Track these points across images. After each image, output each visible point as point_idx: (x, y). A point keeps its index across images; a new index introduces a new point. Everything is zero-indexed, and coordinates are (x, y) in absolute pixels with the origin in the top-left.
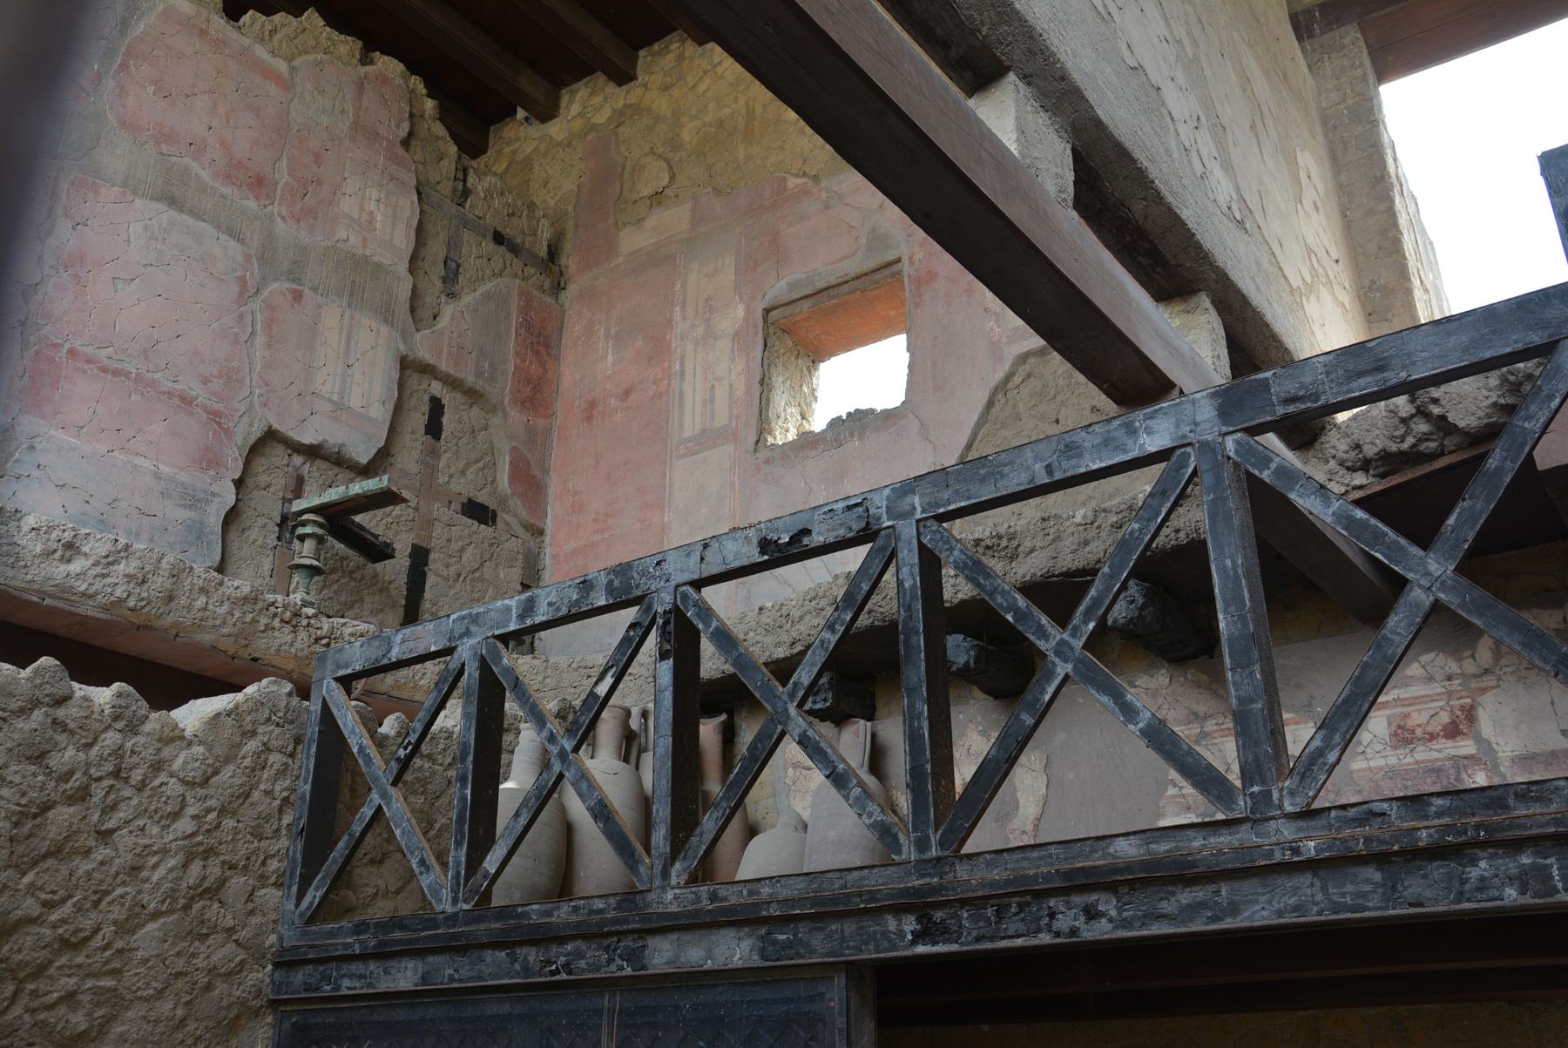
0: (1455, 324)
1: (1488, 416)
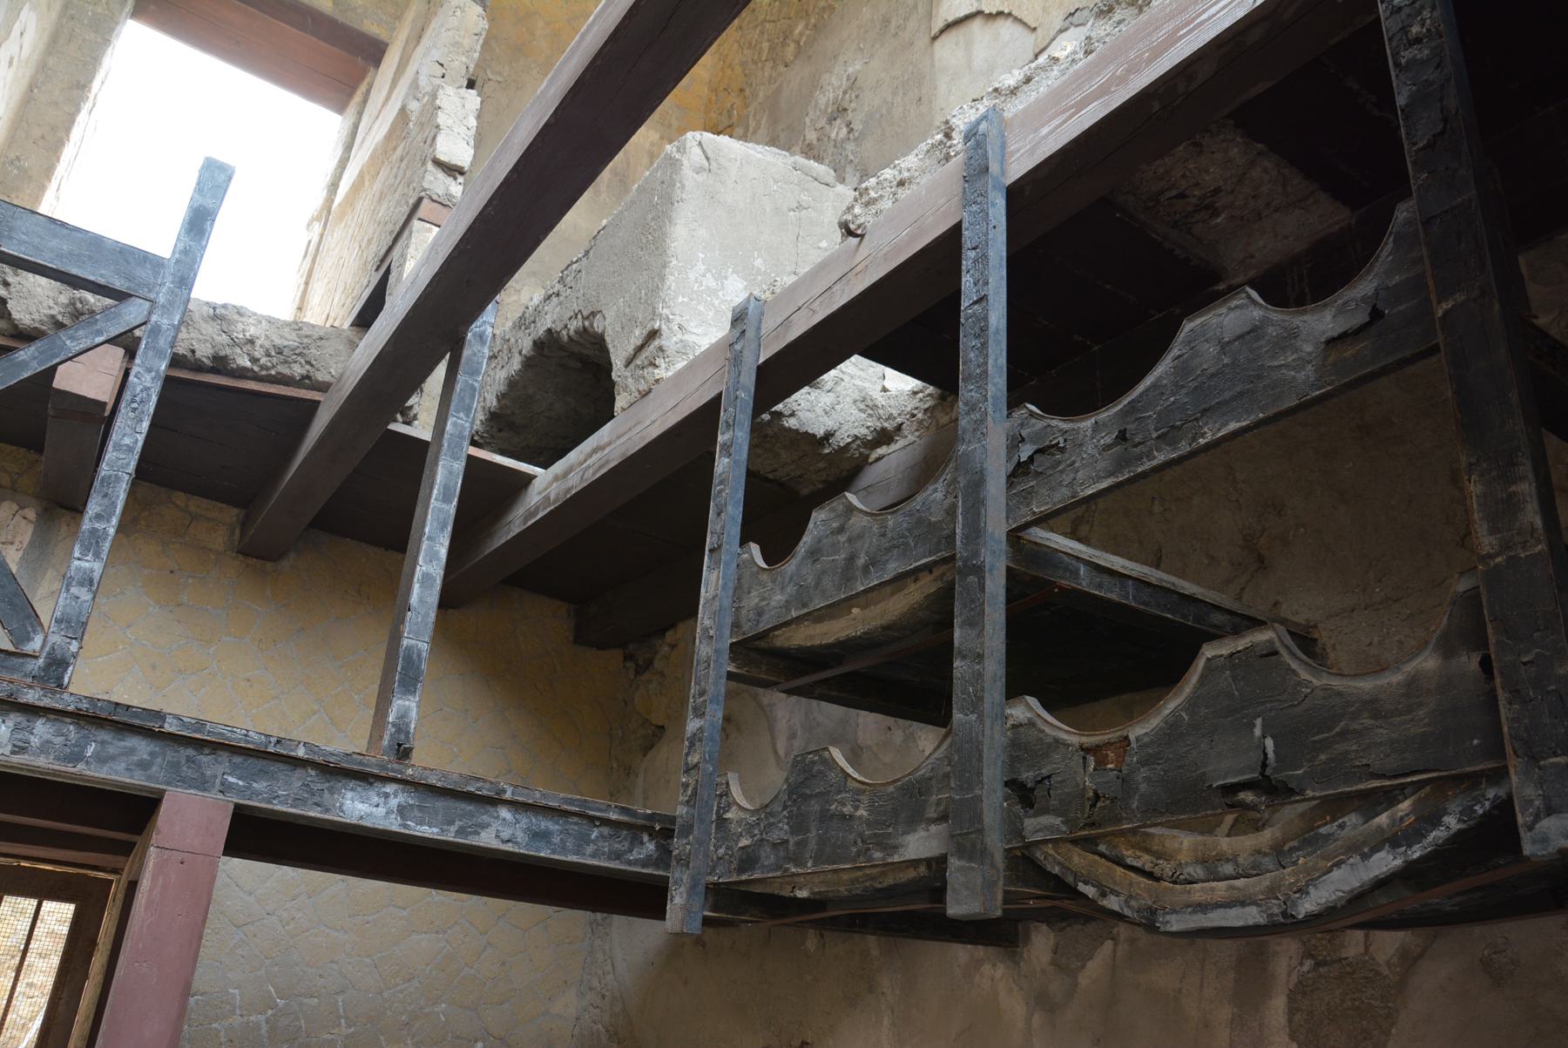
0: (65, 231)
1: (41, 321)
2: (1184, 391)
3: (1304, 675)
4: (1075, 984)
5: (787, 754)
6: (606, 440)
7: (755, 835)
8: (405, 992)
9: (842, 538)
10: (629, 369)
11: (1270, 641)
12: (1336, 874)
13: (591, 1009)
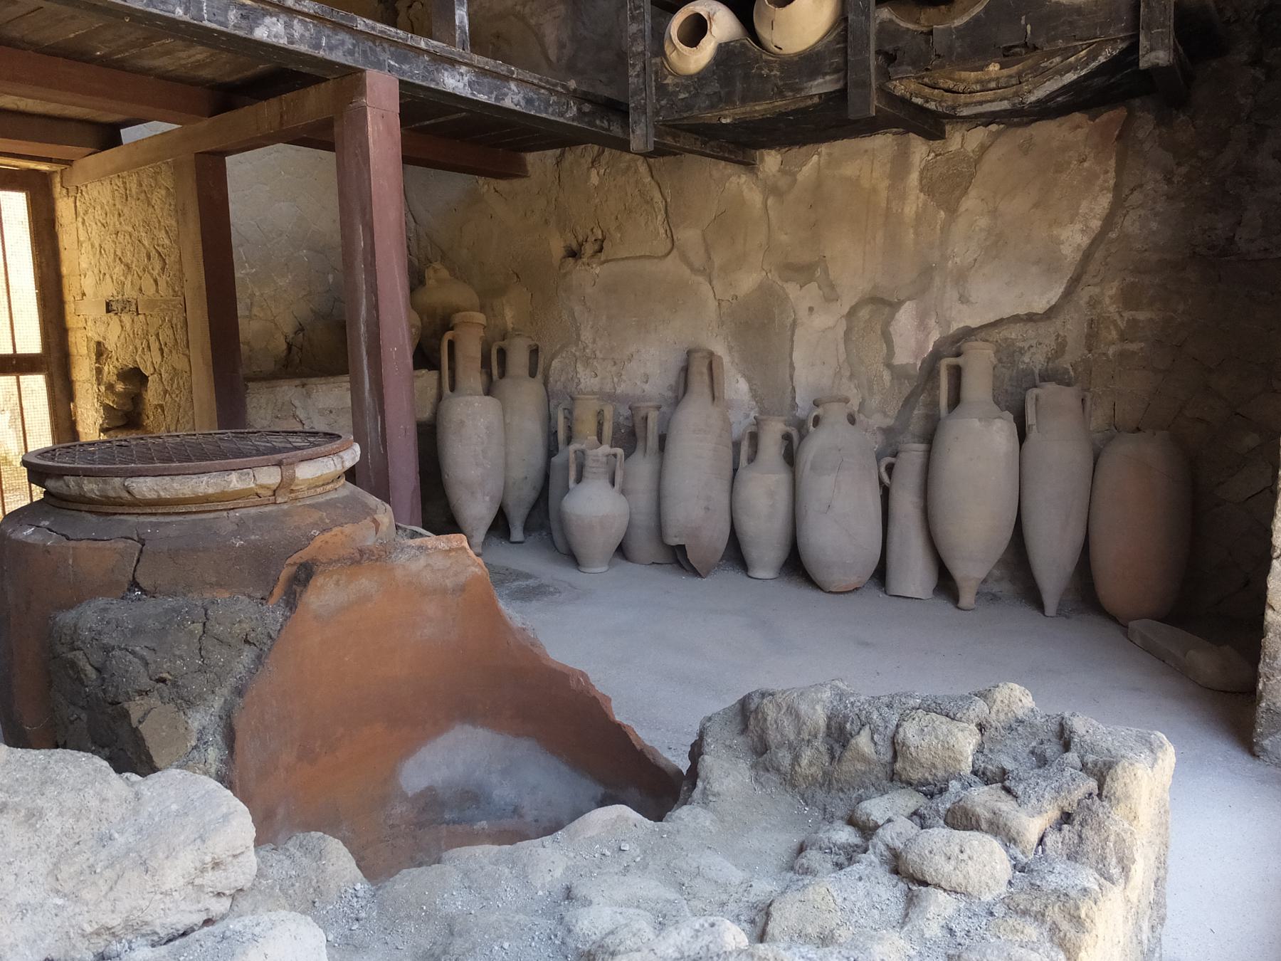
4: (796, 180)
5: (559, 60)
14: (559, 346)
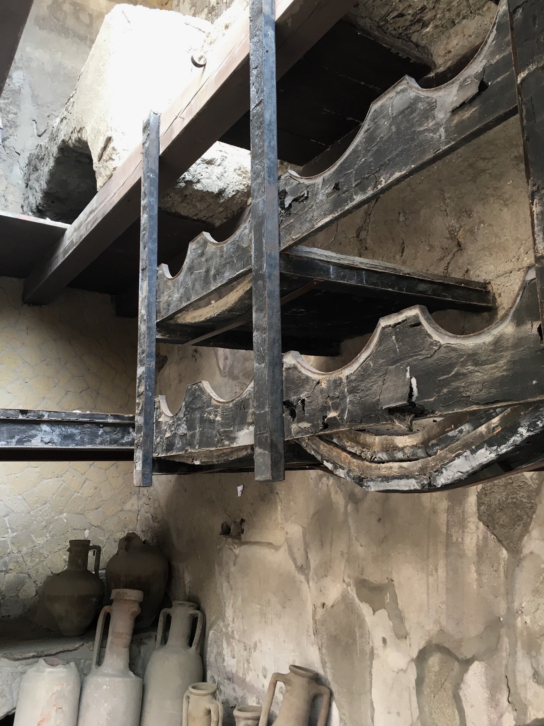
2: (370, 154)
3: (436, 337)
6: (95, 206)
7: (172, 431)
8: (43, 510)
9: (203, 259)
10: (100, 162)
11: (416, 317)
12: (457, 461)
13: (145, 505)
14: (214, 617)
